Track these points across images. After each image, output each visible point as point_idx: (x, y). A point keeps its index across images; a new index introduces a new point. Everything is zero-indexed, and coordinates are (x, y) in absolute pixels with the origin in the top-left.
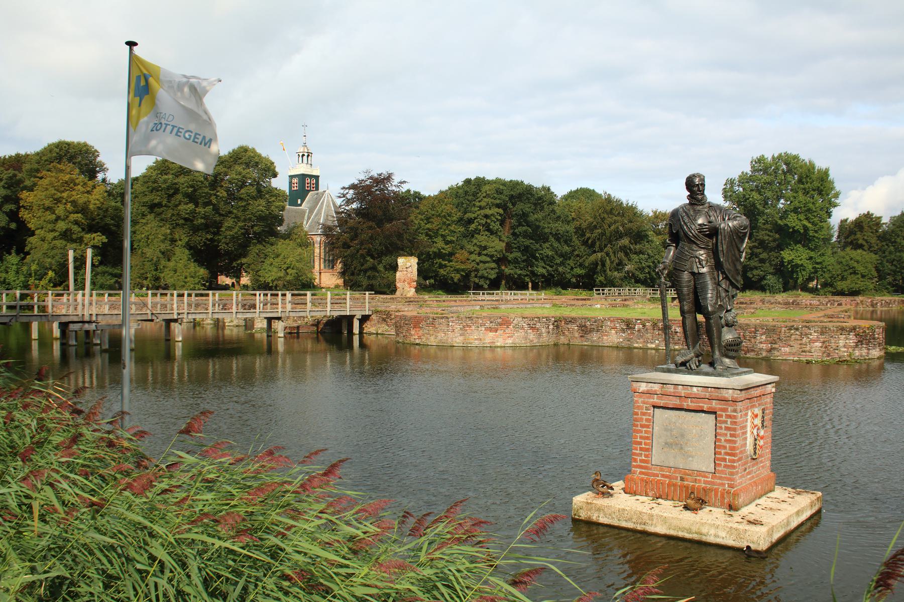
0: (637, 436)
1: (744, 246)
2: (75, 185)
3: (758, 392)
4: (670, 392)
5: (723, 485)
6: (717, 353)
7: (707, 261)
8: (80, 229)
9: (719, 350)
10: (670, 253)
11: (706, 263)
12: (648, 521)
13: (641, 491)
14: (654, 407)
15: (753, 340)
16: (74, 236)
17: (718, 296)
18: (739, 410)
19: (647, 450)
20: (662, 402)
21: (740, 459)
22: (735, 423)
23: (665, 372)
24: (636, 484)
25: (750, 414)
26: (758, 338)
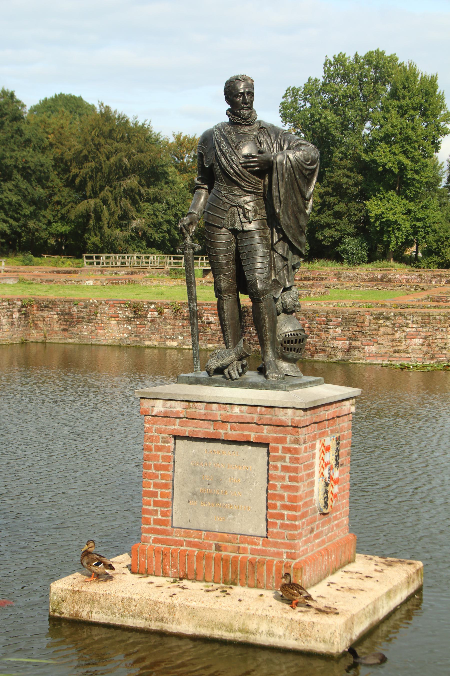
0: (149, 484)
1: (311, 190)
4: (200, 414)
5: (280, 554)
6: (270, 353)
7: (256, 213)
9: (273, 350)
10: (199, 199)
11: (255, 216)
12: (167, 616)
13: (157, 568)
14: (175, 437)
15: (323, 335)
17: (272, 267)
18: (302, 441)
19: (165, 504)
20: (188, 429)
21: (304, 516)
22: (296, 460)
23: (191, 383)
24: (149, 558)
25: (318, 446)
26: (331, 331)
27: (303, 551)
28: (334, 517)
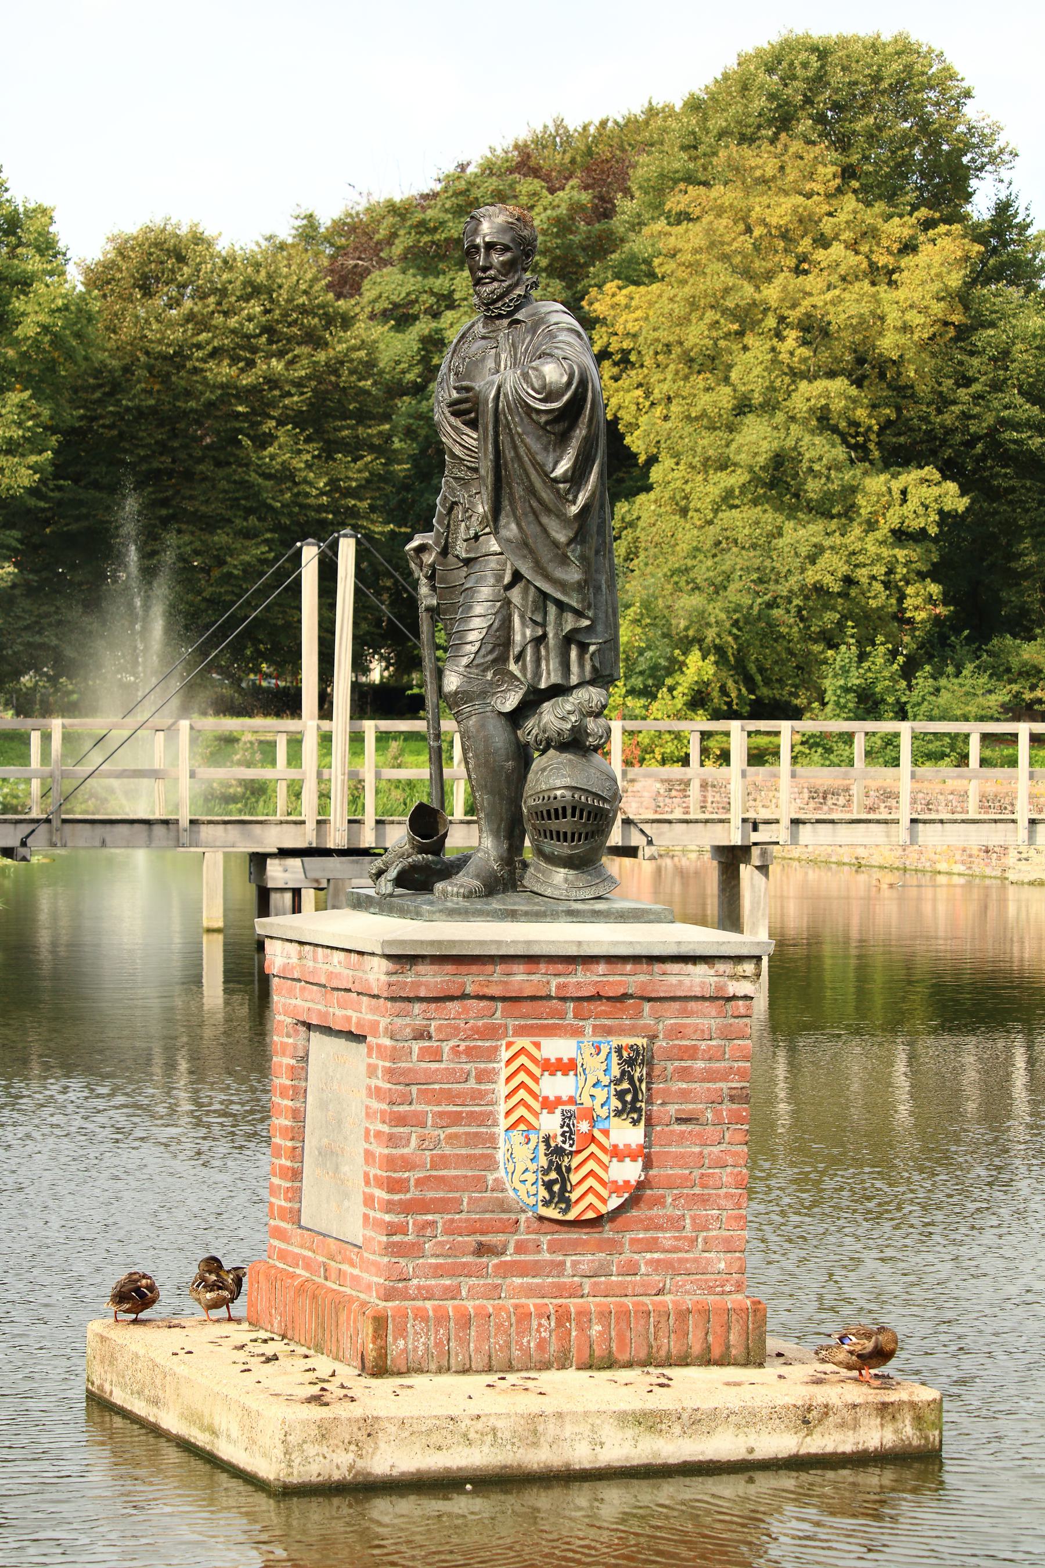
2: (823, 242)
3: (583, 979)
8: (840, 452)
16: (813, 488)
27: (419, 1288)
28: (633, 1241)
